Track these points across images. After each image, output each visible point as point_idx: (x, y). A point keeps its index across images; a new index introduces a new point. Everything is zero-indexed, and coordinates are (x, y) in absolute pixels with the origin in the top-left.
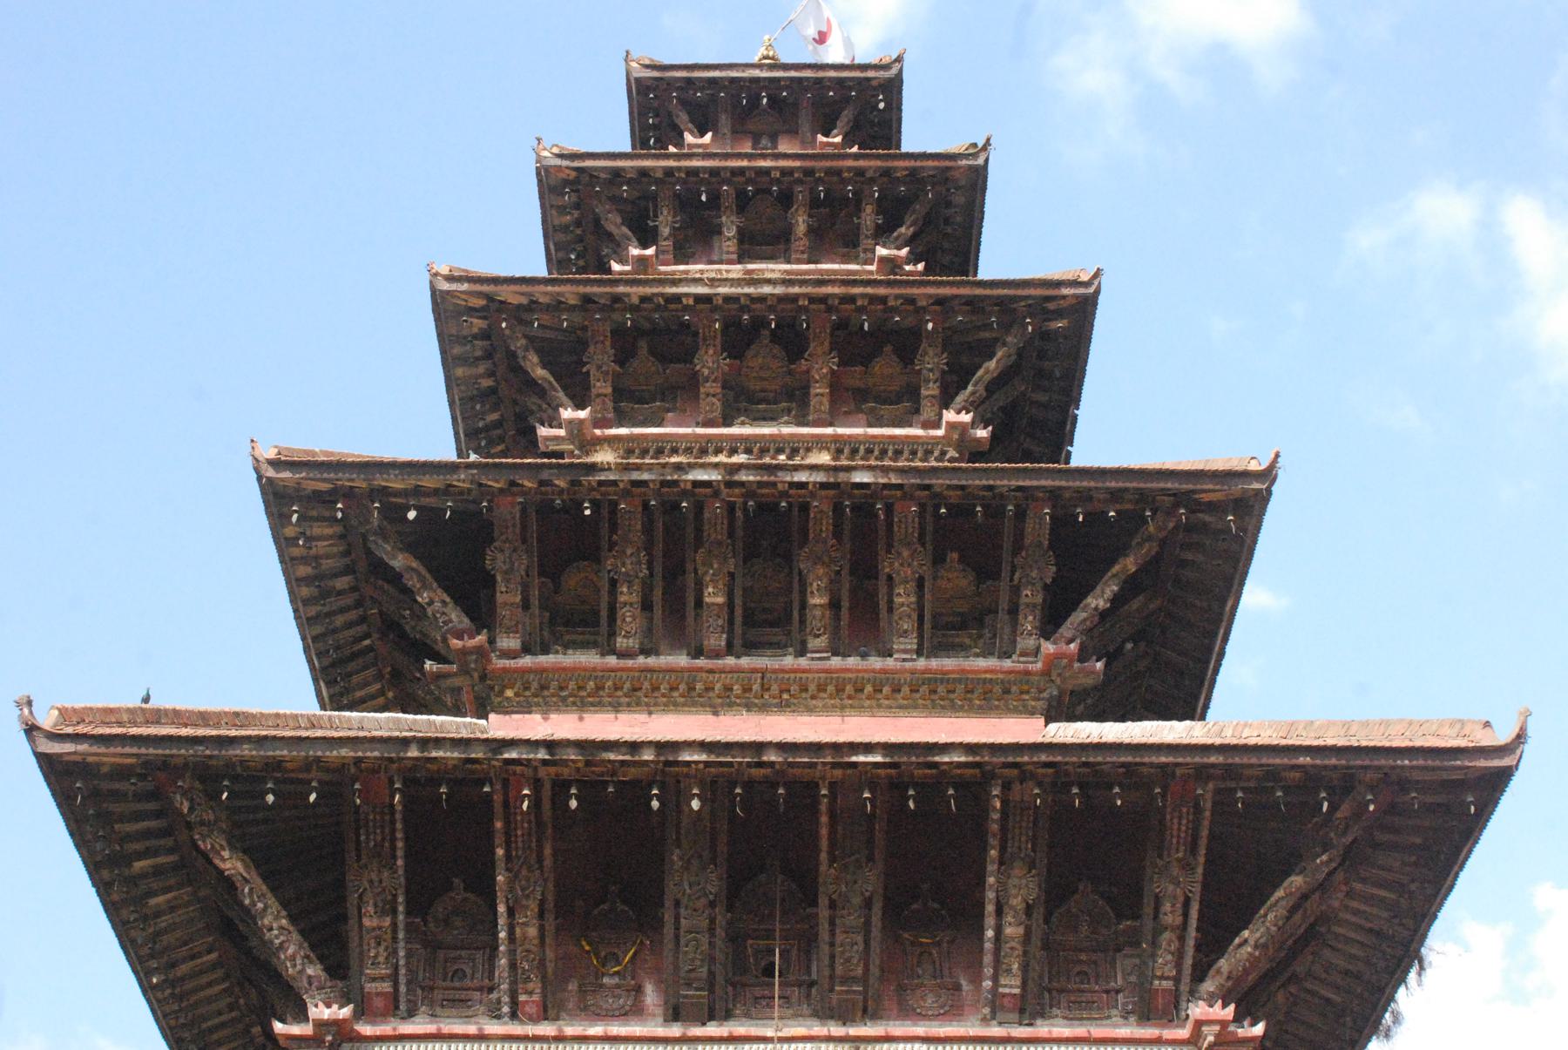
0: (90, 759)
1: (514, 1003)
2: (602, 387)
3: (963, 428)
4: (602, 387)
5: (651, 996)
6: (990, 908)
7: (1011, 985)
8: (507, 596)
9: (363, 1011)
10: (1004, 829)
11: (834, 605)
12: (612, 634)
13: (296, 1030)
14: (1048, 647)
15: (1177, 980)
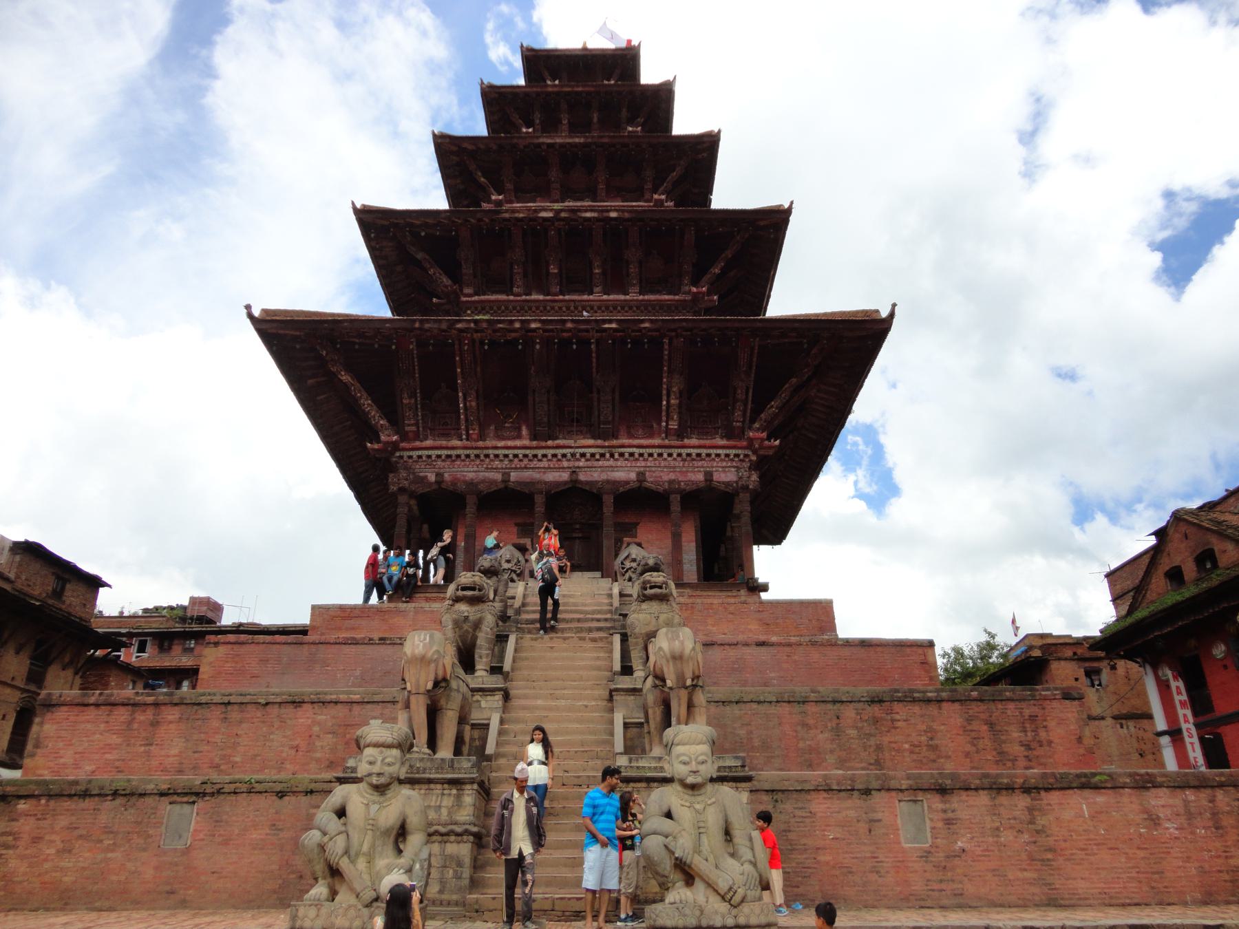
0: (281, 332)
1: (468, 435)
2: (509, 186)
3: (661, 201)
4: (509, 186)
5: (524, 431)
6: (664, 392)
7: (674, 425)
8: (467, 270)
9: (404, 437)
10: (670, 359)
11: (604, 273)
12: (512, 287)
13: (376, 446)
14: (694, 290)
15: (743, 422)
